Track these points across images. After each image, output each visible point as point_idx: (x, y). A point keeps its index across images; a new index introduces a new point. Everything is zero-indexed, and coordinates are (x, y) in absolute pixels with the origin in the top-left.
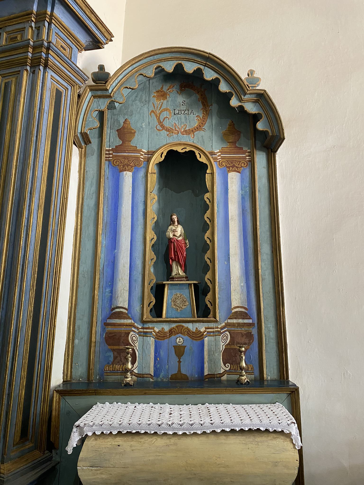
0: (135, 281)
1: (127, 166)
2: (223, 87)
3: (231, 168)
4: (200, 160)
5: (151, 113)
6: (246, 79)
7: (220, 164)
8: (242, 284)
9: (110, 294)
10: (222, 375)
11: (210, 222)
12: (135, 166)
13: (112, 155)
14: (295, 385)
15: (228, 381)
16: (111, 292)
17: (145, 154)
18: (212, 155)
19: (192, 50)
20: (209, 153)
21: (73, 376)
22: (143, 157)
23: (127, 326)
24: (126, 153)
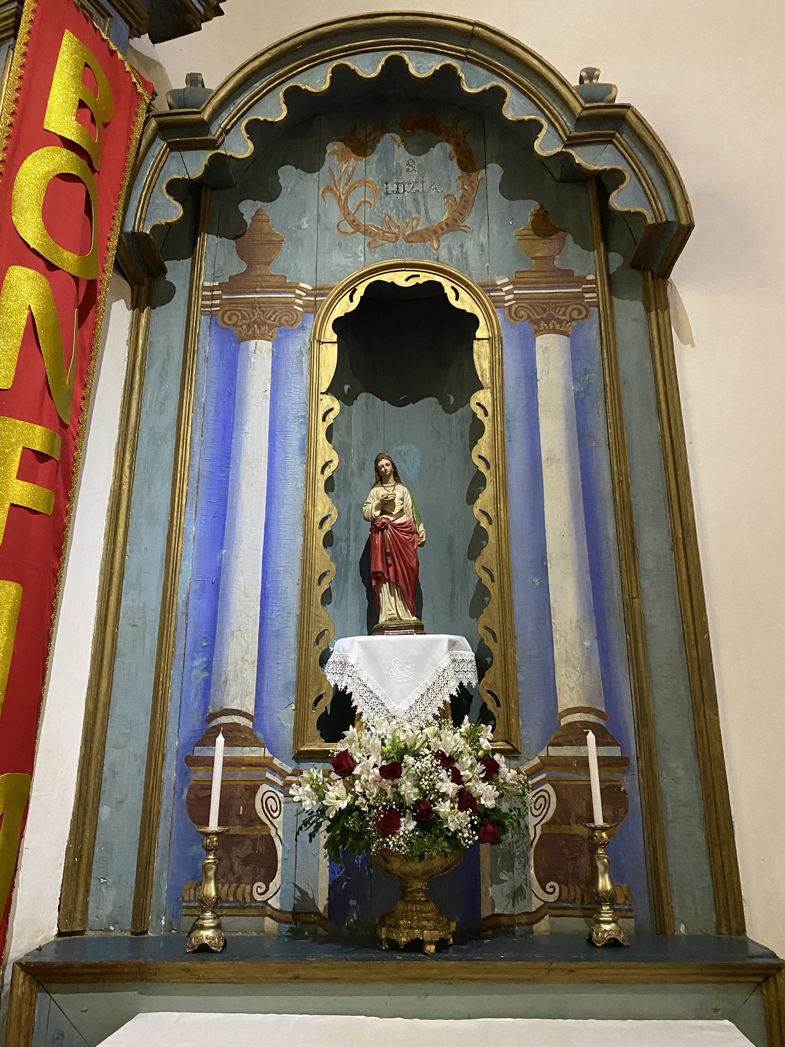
0: (277, 635)
1: (259, 327)
2: (515, 109)
3: (542, 324)
4: (457, 304)
5: (324, 192)
6: (577, 88)
7: (513, 315)
8: (587, 643)
9: (206, 674)
10: (536, 917)
11: (488, 468)
12: (281, 324)
13: (221, 299)
14: (774, 956)
15: (554, 935)
16: (209, 667)
17: (308, 295)
18: (489, 292)
19: (428, 19)
20: (482, 286)
21: (91, 918)
22: (301, 302)
23: (251, 765)
24: (256, 292)
